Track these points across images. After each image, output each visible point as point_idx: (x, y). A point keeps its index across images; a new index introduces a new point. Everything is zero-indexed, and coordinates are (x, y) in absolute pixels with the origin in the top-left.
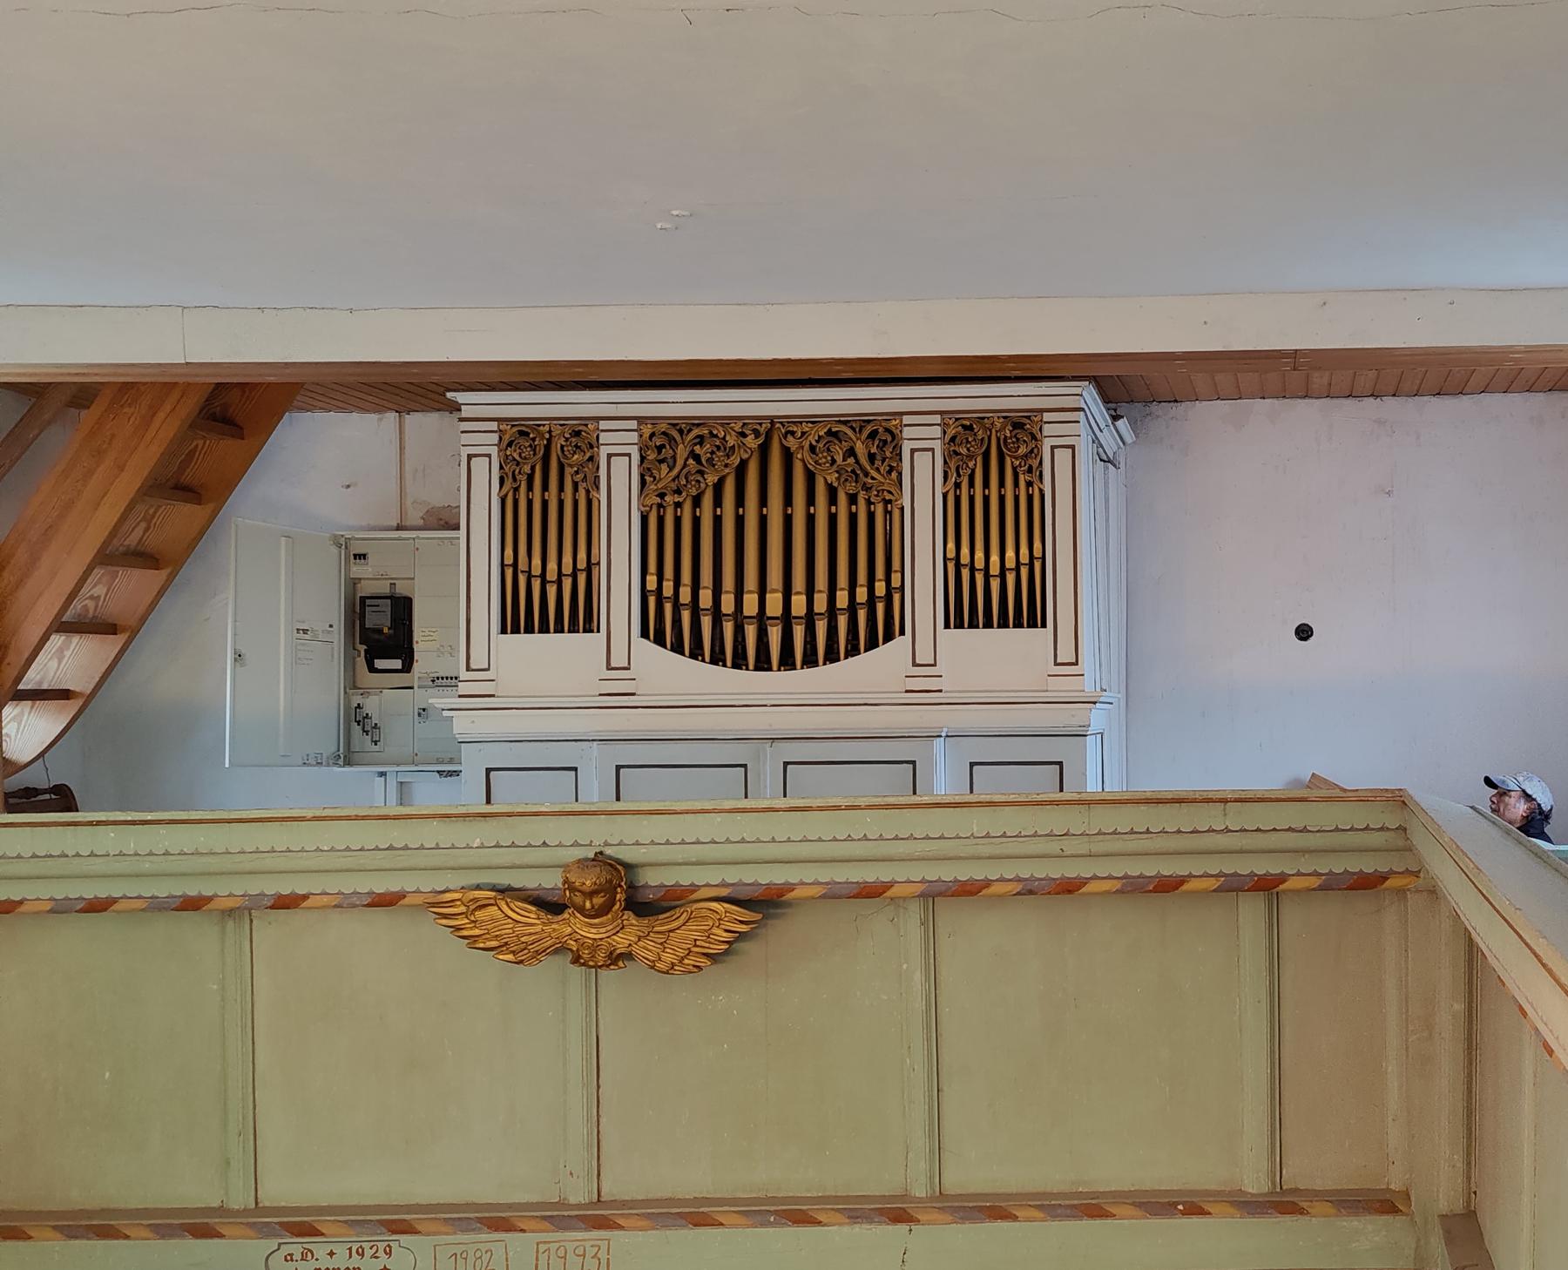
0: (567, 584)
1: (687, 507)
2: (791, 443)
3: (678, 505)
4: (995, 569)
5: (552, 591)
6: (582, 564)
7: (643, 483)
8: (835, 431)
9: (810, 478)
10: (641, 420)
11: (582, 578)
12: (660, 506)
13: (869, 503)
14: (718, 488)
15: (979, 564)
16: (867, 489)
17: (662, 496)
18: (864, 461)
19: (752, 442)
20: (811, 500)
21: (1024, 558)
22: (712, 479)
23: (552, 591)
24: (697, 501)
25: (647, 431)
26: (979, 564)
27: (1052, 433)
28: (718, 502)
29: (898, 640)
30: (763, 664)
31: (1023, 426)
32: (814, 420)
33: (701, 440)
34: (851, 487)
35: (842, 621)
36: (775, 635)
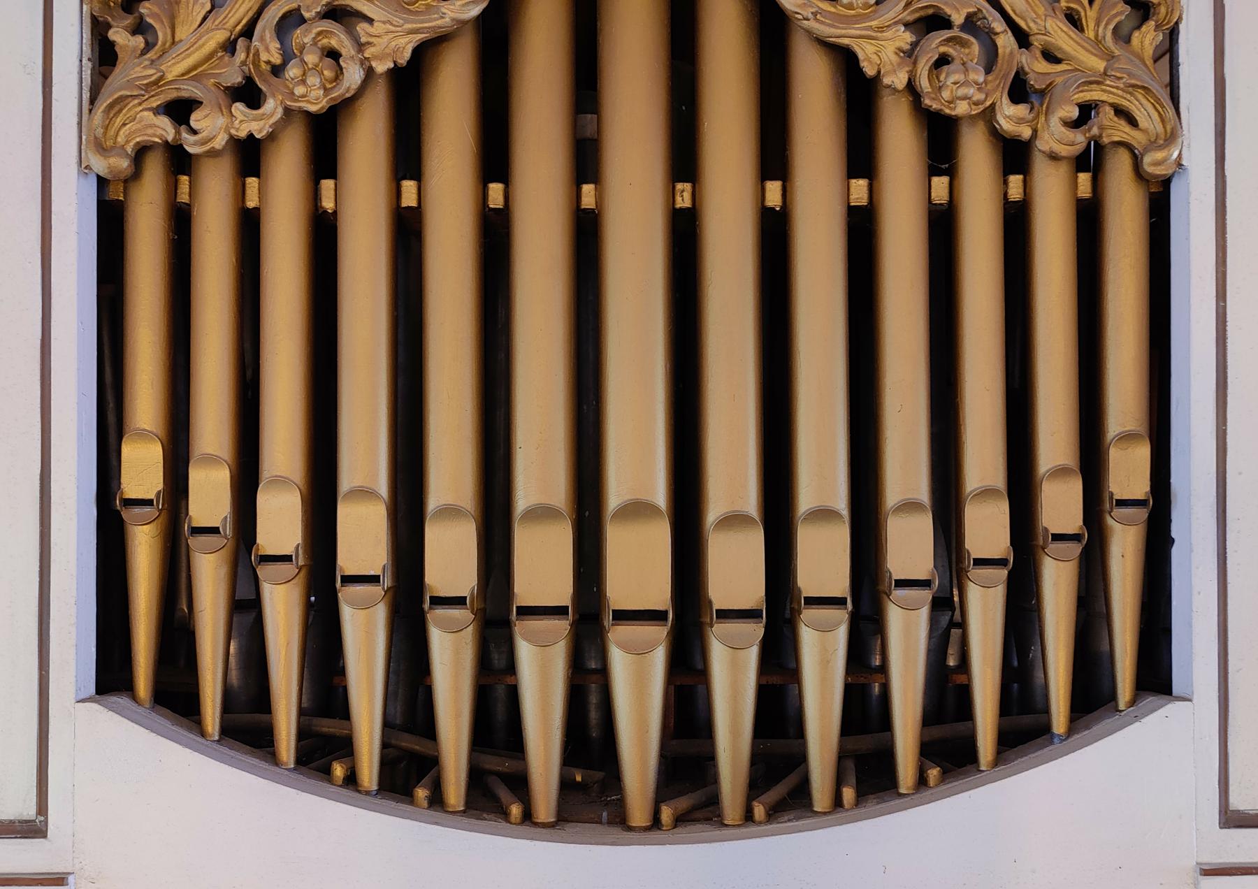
1: (287, 165)
3: (249, 156)
7: (104, 56)
14: (408, 86)
16: (1020, 91)
17: (180, 111)
22: (391, 41)
24: (324, 138)
28: (407, 157)
34: (962, 91)
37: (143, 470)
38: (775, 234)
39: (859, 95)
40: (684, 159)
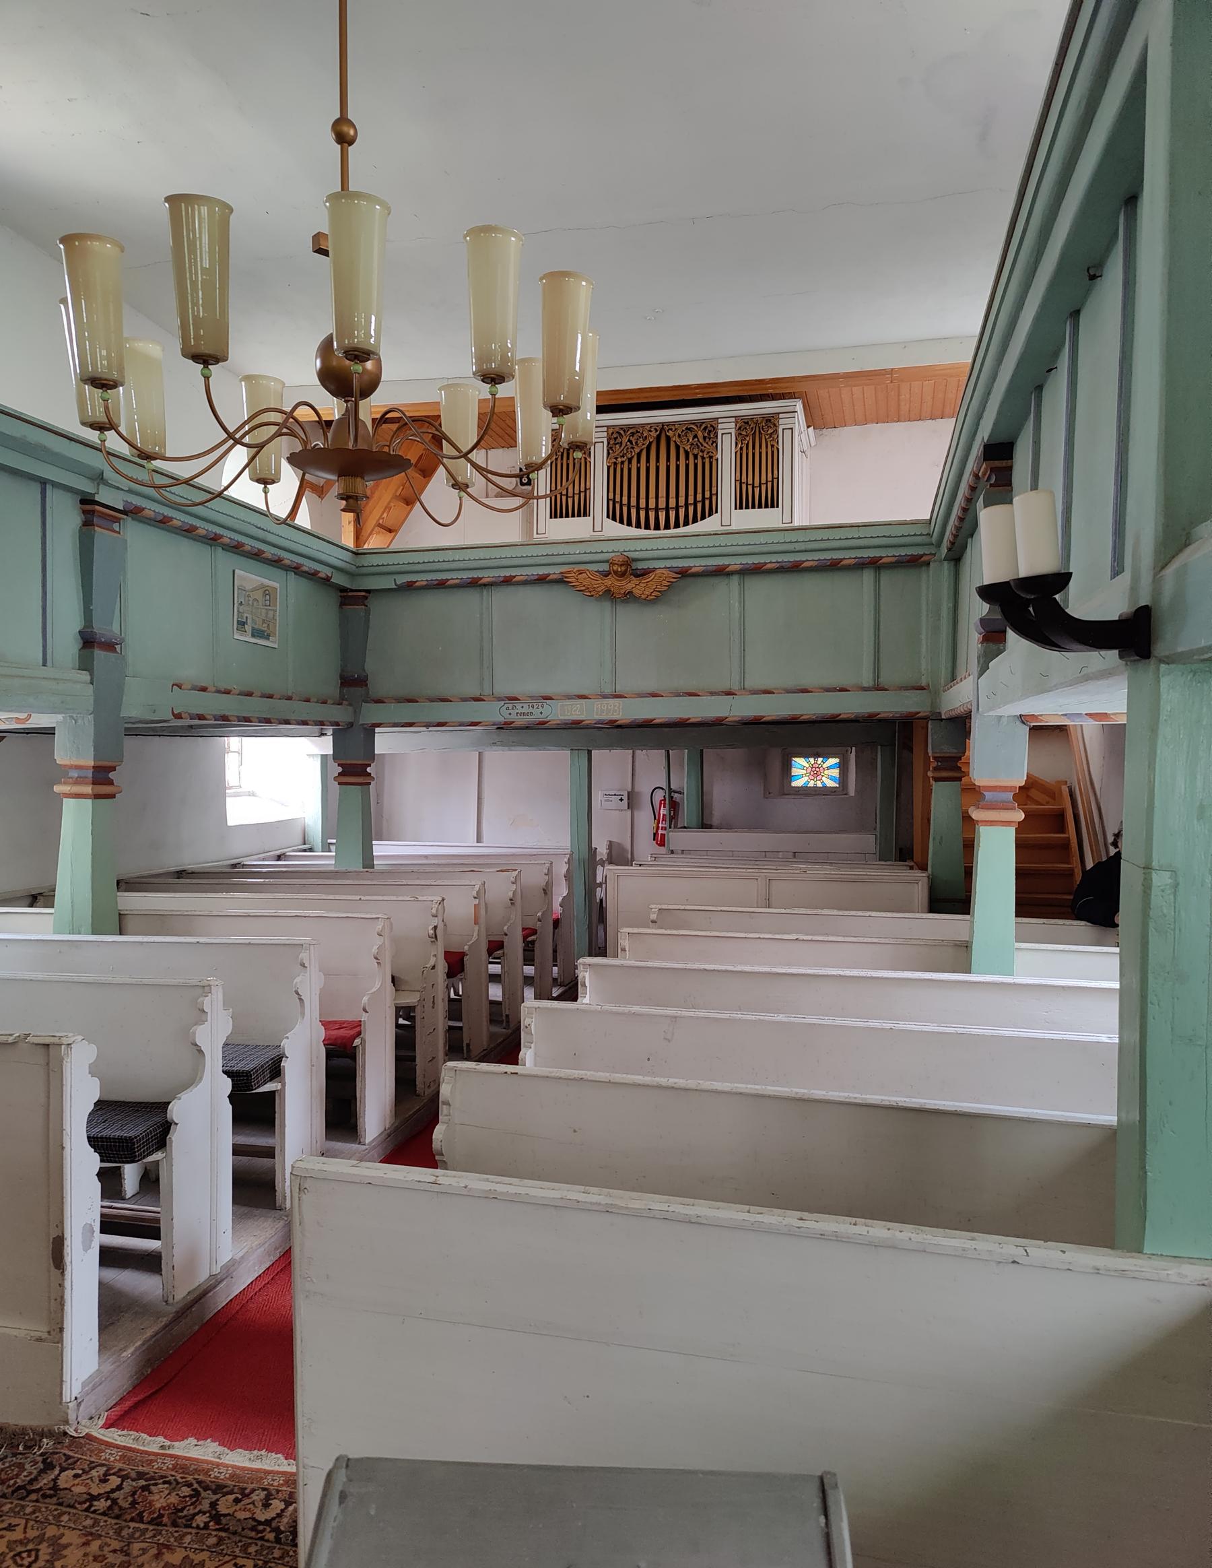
0: (576, 497)
2: (670, 434)
3: (622, 463)
4: (757, 484)
5: (570, 500)
6: (583, 489)
8: (688, 427)
9: (678, 447)
10: (608, 427)
11: (582, 495)
12: (615, 464)
13: (703, 458)
14: (639, 455)
15: (750, 482)
18: (701, 440)
19: (654, 434)
20: (678, 459)
21: (770, 478)
22: (637, 450)
23: (570, 500)
24: (630, 461)
25: (611, 431)
26: (750, 482)
27: (783, 423)
28: (639, 461)
29: (715, 515)
30: (657, 527)
31: (770, 421)
32: (680, 423)
33: (633, 434)
34: (695, 452)
35: (691, 509)
36: (662, 515)
37: (611, 497)
38: (678, 467)
39: (687, 454)
40: (668, 460)
